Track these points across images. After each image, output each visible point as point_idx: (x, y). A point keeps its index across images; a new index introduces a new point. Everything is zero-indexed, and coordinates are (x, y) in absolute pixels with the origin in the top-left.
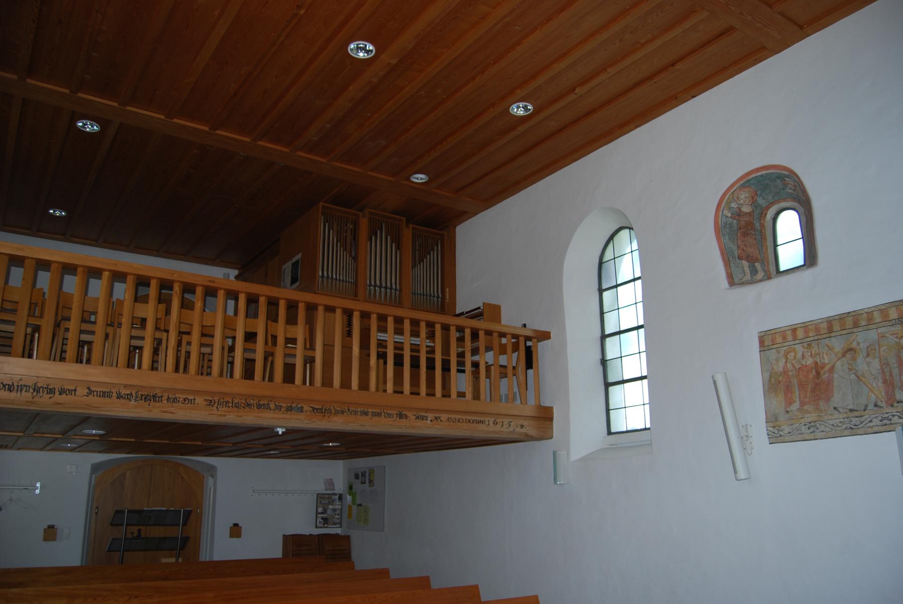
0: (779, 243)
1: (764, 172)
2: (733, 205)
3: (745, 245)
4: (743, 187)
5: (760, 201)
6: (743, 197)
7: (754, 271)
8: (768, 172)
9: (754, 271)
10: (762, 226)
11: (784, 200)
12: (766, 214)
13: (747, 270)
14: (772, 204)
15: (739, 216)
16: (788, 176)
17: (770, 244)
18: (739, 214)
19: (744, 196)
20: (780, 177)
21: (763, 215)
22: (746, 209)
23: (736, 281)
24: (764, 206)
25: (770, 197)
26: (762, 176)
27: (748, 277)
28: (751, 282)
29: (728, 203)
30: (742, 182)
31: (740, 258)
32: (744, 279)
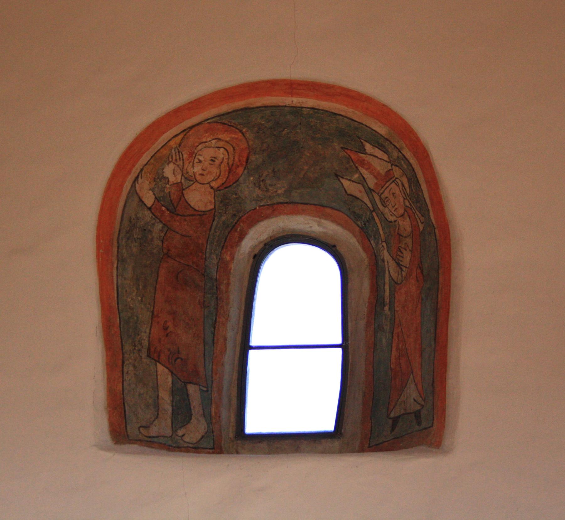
0: (253, 343)
1: (310, 102)
2: (169, 171)
3: (173, 314)
4: (224, 121)
5: (248, 190)
6: (206, 154)
7: (182, 413)
8: (324, 105)
9: (182, 413)
10: (224, 267)
11: (320, 209)
12: (242, 236)
13: (165, 397)
14: (273, 209)
15: (174, 212)
16: (380, 142)
17: (231, 333)
18: (172, 205)
19: (212, 157)
20: (352, 136)
21: (233, 233)
22: (199, 198)
23: (132, 430)
24: (249, 206)
25: (281, 187)
26: (296, 111)
27: (162, 427)
28: (172, 445)
29: (160, 160)
30: (225, 108)
31: (154, 355)
32: (154, 431)
